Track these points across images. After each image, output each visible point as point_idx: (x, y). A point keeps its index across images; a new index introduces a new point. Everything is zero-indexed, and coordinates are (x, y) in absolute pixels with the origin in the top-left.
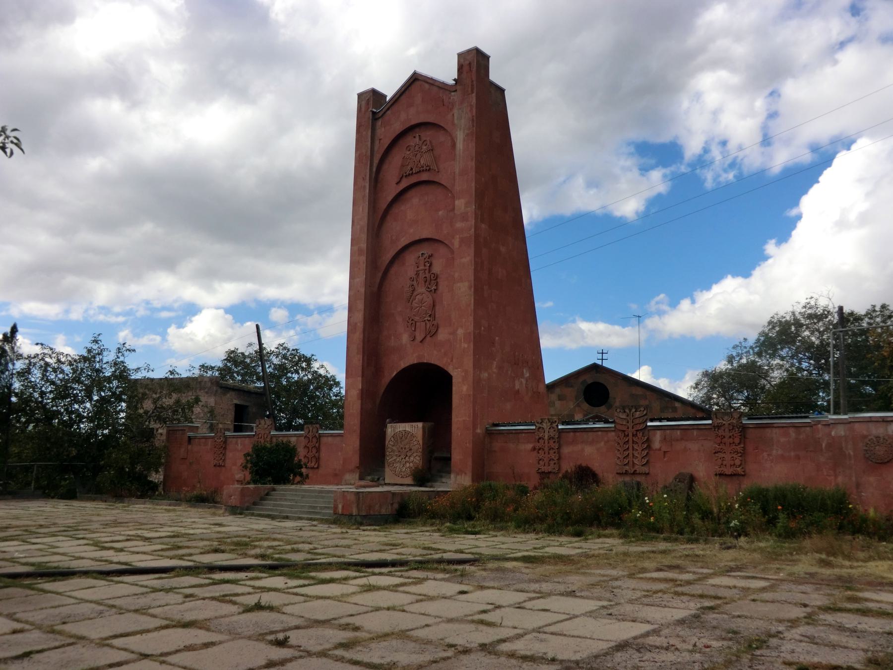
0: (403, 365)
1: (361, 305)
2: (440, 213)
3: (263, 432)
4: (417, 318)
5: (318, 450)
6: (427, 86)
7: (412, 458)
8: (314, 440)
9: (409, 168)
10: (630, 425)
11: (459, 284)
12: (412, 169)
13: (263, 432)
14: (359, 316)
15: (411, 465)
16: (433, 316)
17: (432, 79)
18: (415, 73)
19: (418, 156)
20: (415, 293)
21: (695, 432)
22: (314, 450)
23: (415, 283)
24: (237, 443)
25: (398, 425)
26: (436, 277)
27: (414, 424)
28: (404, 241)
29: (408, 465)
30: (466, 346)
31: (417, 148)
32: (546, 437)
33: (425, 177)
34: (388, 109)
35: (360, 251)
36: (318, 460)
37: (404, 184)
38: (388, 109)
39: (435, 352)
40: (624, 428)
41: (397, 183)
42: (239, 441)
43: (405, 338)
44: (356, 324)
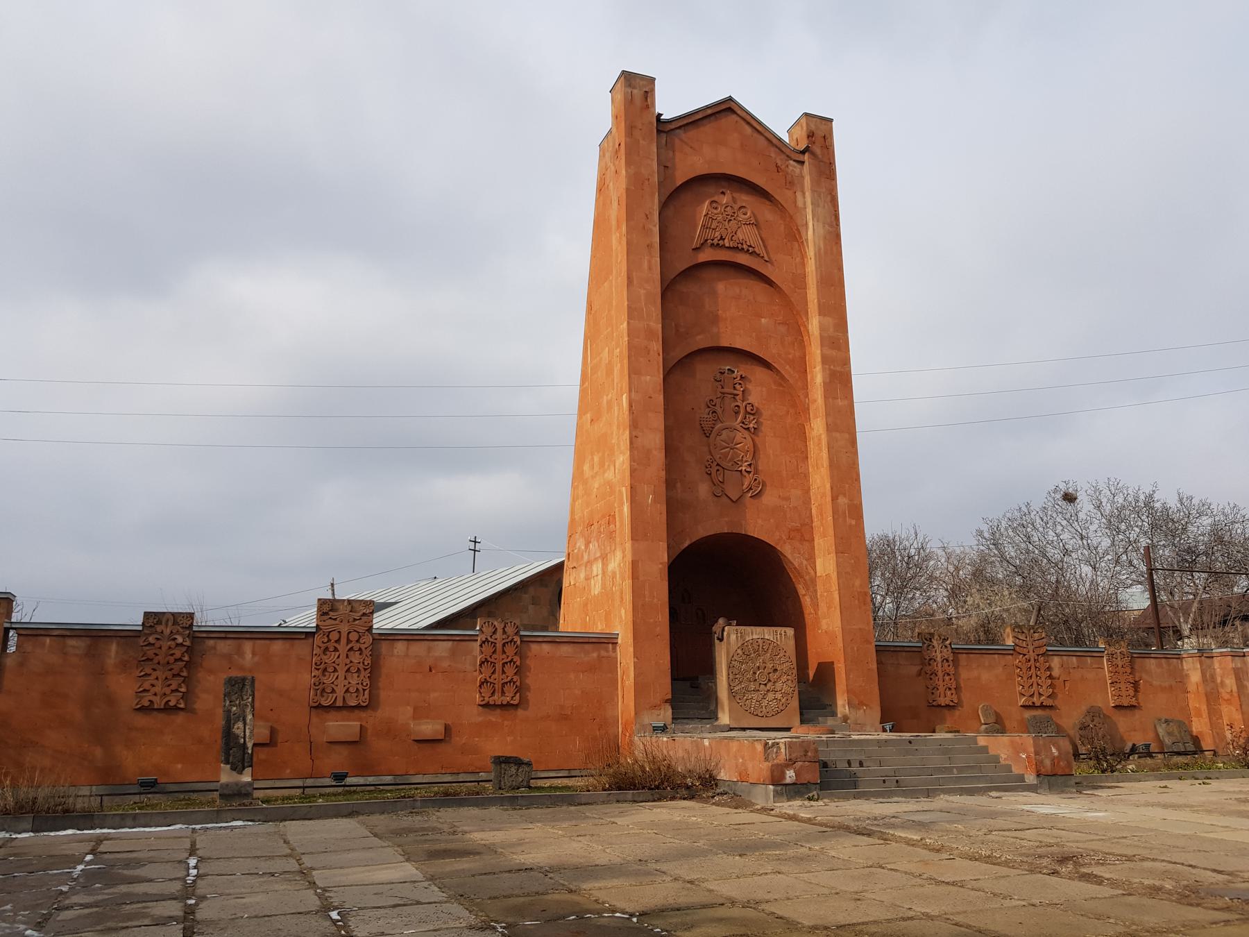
1: (658, 421)
3: (345, 629)
4: (724, 464)
5: (519, 671)
6: (748, 130)
7: (779, 685)
8: (510, 650)
10: (1031, 648)
12: (722, 239)
13: (345, 629)
14: (655, 440)
15: (779, 696)
16: (754, 467)
17: (760, 123)
18: (730, 99)
20: (719, 426)
21: (1089, 659)
22: (510, 671)
23: (718, 409)
24: (240, 652)
25: (749, 629)
26: (754, 412)
27: (779, 629)
28: (702, 341)
29: (771, 696)
30: (853, 522)
32: (939, 659)
33: (742, 259)
35: (650, 333)
36: (521, 689)
38: (680, 127)
39: (760, 521)
40: (1025, 651)
42: (248, 646)
43: (704, 489)
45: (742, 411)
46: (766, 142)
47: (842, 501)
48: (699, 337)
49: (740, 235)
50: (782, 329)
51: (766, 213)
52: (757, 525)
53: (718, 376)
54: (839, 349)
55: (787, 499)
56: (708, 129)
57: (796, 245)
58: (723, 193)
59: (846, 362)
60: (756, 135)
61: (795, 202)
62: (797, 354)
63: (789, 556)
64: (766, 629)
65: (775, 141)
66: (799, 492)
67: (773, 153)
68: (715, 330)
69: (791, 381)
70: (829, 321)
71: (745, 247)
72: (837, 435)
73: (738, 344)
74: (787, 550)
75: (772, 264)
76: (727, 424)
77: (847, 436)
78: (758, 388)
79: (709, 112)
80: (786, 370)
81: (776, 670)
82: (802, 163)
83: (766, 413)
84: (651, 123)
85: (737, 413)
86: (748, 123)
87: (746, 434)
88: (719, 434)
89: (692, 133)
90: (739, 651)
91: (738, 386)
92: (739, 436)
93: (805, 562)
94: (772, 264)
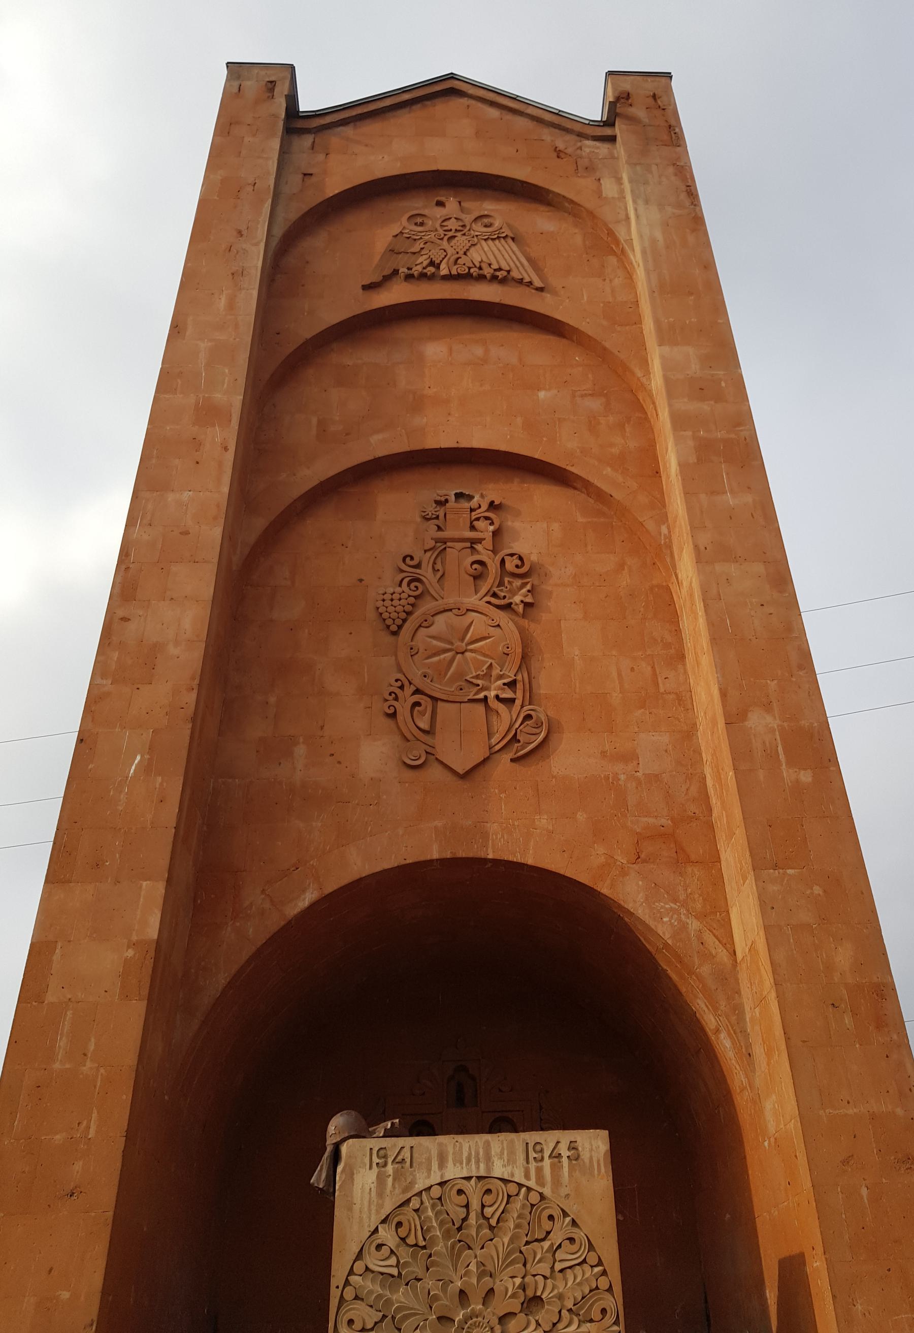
0: (359, 862)
2: (542, 394)
4: (436, 689)
6: (494, 113)
9: (423, 260)
11: (719, 568)
12: (432, 263)
16: (520, 687)
18: (452, 77)
19: (461, 242)
20: (427, 606)
23: (426, 573)
26: (525, 572)
27: (549, 1139)
28: (381, 444)
31: (452, 224)
34: (344, 122)
37: (398, 294)
41: (365, 288)
43: (375, 755)
44: (156, 649)
45: (493, 567)
46: (529, 124)
47: (760, 723)
48: (375, 439)
49: (476, 256)
50: (595, 404)
51: (540, 222)
52: (525, 829)
53: (431, 509)
54: (719, 398)
55: (630, 757)
56: (405, 118)
57: (613, 260)
58: (440, 204)
59: (743, 419)
60: (509, 117)
61: (599, 193)
62: (632, 444)
63: (642, 912)
64: (498, 1142)
65: (548, 117)
66: (664, 739)
67: (547, 135)
68: (419, 421)
69: (617, 495)
70: (689, 356)
71: (487, 271)
72: (732, 569)
73: (478, 439)
74: (633, 894)
75: (555, 293)
76: (450, 601)
77: (759, 568)
78: (536, 525)
79: (406, 97)
80: (604, 477)
81: (533, 1302)
82: (612, 139)
83: (560, 575)
84: (275, 116)
85: (477, 578)
86: (493, 104)
87: (502, 617)
88: (425, 623)
89: (372, 128)
90: (387, 1235)
91: (480, 524)
92: (479, 624)
93: (694, 925)
94: (555, 293)
